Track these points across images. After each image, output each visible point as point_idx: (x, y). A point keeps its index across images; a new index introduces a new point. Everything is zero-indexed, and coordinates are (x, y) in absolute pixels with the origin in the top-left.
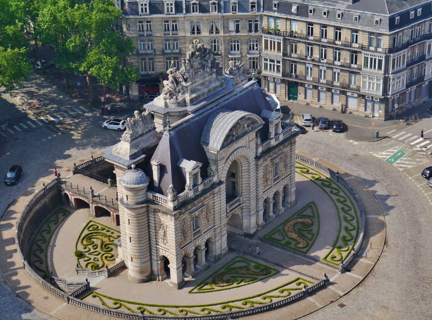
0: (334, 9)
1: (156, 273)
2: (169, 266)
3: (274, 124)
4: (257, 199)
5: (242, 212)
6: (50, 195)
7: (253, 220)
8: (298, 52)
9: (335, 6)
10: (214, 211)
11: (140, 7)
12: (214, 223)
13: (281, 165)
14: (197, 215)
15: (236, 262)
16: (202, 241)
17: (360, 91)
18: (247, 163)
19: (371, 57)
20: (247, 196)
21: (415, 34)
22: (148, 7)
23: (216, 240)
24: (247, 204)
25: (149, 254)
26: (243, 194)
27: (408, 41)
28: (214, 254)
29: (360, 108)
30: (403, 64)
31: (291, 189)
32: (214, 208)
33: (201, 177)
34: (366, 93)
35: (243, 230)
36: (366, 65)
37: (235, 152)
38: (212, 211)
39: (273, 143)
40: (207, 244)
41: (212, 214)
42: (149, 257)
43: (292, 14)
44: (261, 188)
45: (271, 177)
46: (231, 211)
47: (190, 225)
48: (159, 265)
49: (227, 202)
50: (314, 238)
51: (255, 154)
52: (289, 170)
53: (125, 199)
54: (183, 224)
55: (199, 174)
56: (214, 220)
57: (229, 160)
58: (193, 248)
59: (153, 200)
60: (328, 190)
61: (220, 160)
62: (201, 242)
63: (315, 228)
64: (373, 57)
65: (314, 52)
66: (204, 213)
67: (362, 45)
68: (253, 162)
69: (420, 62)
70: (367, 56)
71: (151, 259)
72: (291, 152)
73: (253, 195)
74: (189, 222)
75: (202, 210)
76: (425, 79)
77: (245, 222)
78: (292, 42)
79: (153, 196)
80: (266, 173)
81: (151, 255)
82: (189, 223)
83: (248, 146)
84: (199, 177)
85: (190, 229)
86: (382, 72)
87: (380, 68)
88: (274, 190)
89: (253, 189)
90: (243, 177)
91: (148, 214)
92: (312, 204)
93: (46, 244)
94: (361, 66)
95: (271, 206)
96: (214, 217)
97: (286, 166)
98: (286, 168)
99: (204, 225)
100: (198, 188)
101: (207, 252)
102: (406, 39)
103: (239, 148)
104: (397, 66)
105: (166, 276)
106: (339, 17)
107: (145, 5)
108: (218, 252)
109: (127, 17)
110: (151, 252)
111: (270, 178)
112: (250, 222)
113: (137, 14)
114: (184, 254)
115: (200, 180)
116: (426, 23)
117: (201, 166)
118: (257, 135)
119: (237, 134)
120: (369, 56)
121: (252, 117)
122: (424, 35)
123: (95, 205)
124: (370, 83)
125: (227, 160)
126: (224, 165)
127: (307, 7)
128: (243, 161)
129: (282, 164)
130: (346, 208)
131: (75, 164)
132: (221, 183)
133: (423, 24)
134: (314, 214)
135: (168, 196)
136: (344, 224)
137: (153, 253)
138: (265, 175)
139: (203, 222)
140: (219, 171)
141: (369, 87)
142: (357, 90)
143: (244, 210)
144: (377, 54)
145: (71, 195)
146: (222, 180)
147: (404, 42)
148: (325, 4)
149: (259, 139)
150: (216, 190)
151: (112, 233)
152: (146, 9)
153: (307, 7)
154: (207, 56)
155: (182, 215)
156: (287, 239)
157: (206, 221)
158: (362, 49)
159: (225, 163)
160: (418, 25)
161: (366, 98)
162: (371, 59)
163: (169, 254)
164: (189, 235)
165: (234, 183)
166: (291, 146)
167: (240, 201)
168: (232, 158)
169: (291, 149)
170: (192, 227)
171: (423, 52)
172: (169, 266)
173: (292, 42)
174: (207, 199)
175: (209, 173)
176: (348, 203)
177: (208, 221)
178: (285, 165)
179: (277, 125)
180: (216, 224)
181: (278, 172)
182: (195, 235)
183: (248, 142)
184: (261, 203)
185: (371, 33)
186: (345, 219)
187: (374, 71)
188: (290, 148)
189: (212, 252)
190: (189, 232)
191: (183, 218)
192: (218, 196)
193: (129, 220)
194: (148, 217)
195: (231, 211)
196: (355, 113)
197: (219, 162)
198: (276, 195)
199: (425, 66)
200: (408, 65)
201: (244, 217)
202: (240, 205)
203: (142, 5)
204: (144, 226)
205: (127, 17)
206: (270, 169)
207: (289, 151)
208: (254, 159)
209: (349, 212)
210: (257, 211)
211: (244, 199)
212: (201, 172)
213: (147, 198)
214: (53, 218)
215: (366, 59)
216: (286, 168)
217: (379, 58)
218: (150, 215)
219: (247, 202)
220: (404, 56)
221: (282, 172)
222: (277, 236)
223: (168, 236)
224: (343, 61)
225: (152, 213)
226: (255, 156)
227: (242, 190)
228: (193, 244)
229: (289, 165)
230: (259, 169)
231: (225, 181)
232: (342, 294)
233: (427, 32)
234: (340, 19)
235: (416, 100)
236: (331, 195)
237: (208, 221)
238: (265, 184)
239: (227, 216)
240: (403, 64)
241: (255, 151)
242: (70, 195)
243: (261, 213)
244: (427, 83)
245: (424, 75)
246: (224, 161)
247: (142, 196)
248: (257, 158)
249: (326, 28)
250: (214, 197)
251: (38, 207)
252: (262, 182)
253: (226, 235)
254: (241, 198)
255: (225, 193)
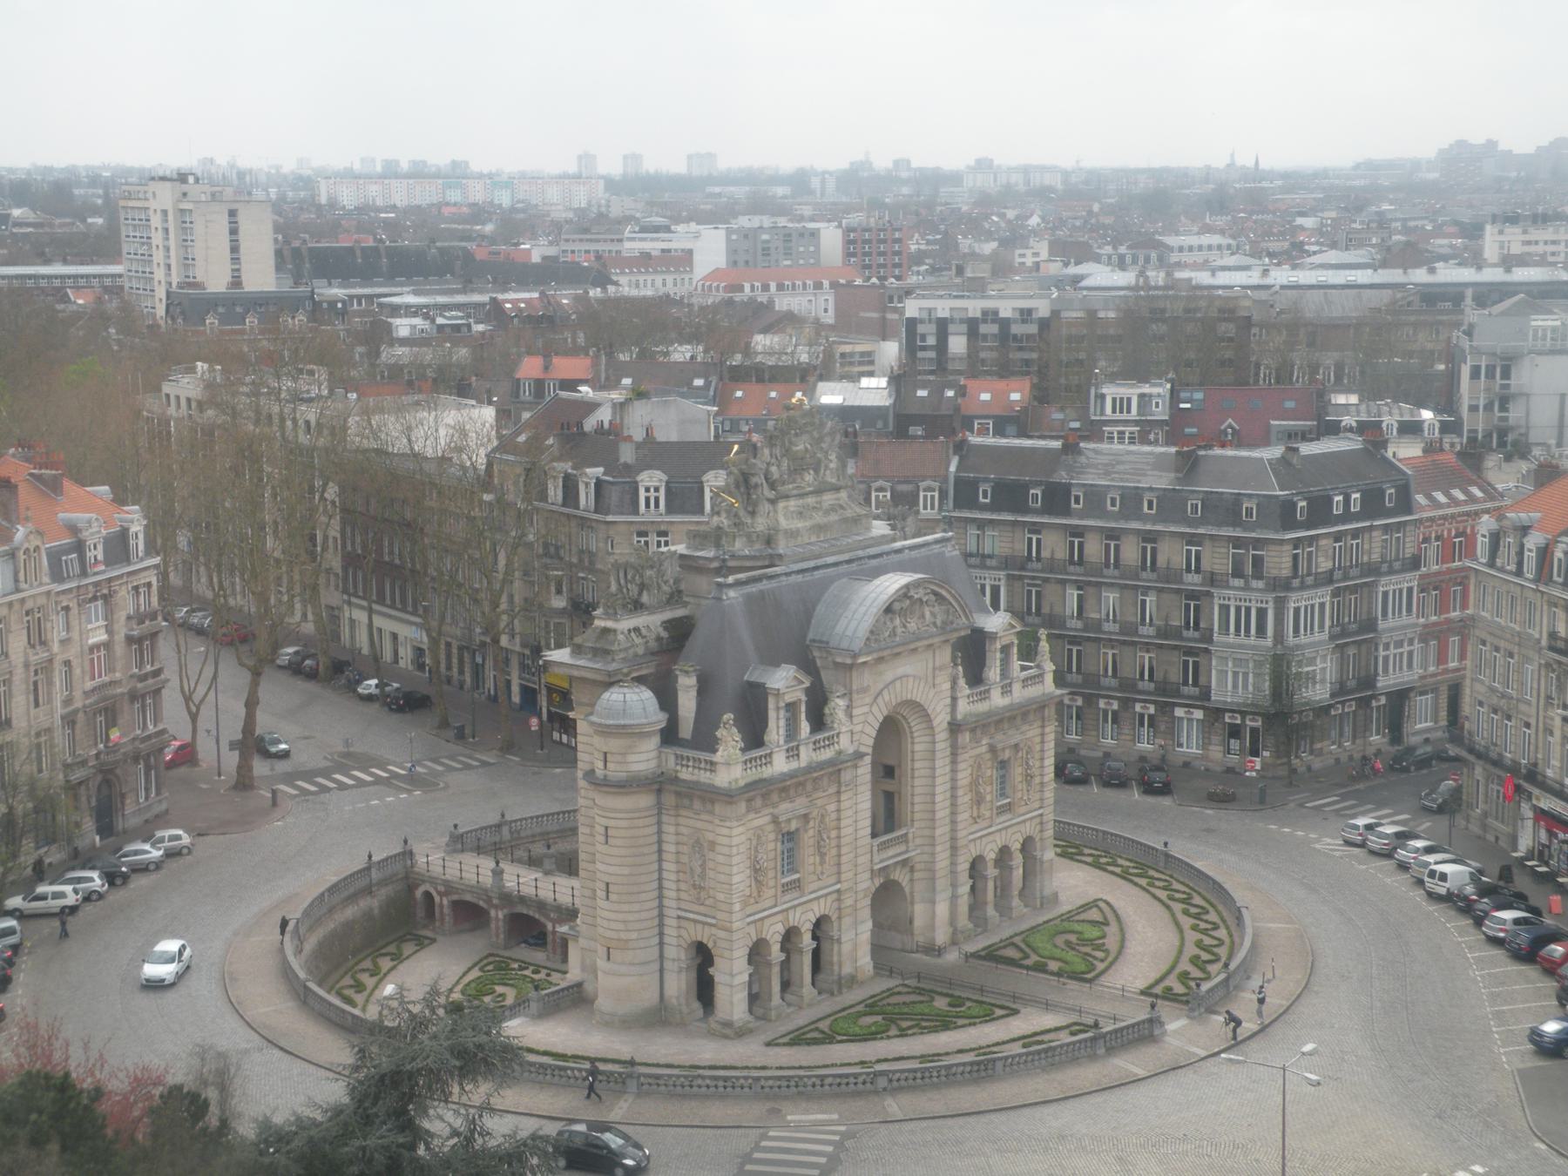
0: (1137, 488)
1: (674, 1001)
2: (711, 971)
3: (998, 646)
4: (954, 849)
5: (911, 880)
6: (384, 893)
7: (942, 909)
8: (1046, 610)
9: (1139, 482)
10: (839, 837)
11: (642, 494)
12: (839, 873)
13: (1017, 771)
14: (794, 826)
15: (899, 993)
16: (803, 918)
17: (1209, 699)
18: (927, 732)
19: (1238, 603)
20: (927, 832)
21: (1348, 558)
22: (662, 494)
23: (843, 927)
24: (926, 858)
25: (656, 940)
26: (916, 824)
27: (1331, 572)
28: (836, 968)
29: (1211, 748)
30: (1322, 626)
31: (1043, 849)
32: (839, 828)
33: (808, 719)
34: (1226, 702)
35: (912, 934)
36: (1225, 629)
37: (898, 684)
38: (833, 834)
39: (998, 700)
40: (819, 925)
41: (834, 843)
42: (657, 948)
43: (1026, 510)
44: (963, 816)
45: (989, 792)
46: (881, 861)
47: (772, 855)
48: (683, 976)
49: (874, 835)
50: (1110, 959)
51: (948, 710)
52: (1037, 796)
53: (600, 764)
54: (754, 842)
55: (803, 708)
56: (839, 864)
57: (880, 700)
58: (780, 928)
59: (677, 771)
60: (1143, 882)
61: (858, 692)
62: (804, 920)
63: (1111, 942)
64: (1243, 603)
65: (1087, 606)
66: (811, 833)
67: (1212, 573)
68: (942, 735)
69: (1363, 634)
70: (1226, 602)
71: (661, 956)
72: (1043, 742)
73: (942, 831)
74: (772, 847)
75: (806, 818)
76: (1379, 685)
77: (919, 910)
78: (1029, 585)
79: (677, 756)
80: (977, 779)
81: (661, 944)
82: (771, 846)
83: (930, 679)
84: (803, 716)
85: (772, 864)
86: (1269, 642)
87: (1261, 630)
88: (1000, 841)
89: (942, 813)
90: (917, 773)
91: (659, 814)
92: (1102, 905)
93: (366, 993)
94: (1212, 630)
95: (991, 885)
96: (839, 856)
97: (1028, 778)
98: (1029, 784)
99: (812, 868)
100: (797, 747)
101: (816, 954)
102: (1324, 565)
103: (908, 676)
104: (1305, 630)
105: (700, 1012)
106: (1150, 507)
107: (657, 490)
108: (847, 969)
109: (610, 518)
110: (661, 925)
111: (988, 798)
112: (934, 912)
113: (636, 512)
114: (755, 939)
115: (805, 727)
116: (1375, 534)
117: (807, 684)
118: (954, 659)
119: (905, 626)
120: (1232, 603)
121: (944, 593)
122: (1369, 564)
123: (505, 911)
124: (1235, 674)
125: (876, 698)
126: (866, 709)
127: (1066, 489)
128: (915, 725)
129: (1019, 770)
130: (1193, 910)
131: (456, 826)
132: (859, 756)
133: (1367, 536)
134: (1105, 918)
135: (715, 751)
136: (1191, 936)
137: (667, 940)
138: (974, 784)
139: (808, 857)
140: (855, 720)
141: (1235, 686)
142: (1202, 700)
143: (917, 875)
144: (1254, 596)
145: (440, 894)
146: (863, 749)
147: (1319, 570)
148: (1112, 480)
149: (960, 668)
150: (846, 776)
151: (548, 975)
152: (657, 500)
153: (1066, 489)
154: (828, 439)
155: (752, 816)
156: (1034, 958)
157: (818, 858)
158: (1212, 585)
159: (871, 705)
160: (1356, 534)
161: (1227, 720)
162: (1238, 609)
163: (714, 930)
164: (772, 883)
165: (889, 797)
166: (1043, 727)
167: (907, 842)
168: (889, 699)
169: (1043, 735)
170: (779, 859)
171: (1369, 612)
172: (711, 971)
173: (1029, 585)
174: (821, 794)
175: (828, 720)
176: (1197, 900)
177: (822, 863)
178: (1027, 775)
179: (1006, 649)
180: (844, 877)
181: (1008, 791)
182: (787, 888)
183: (930, 670)
184: (963, 866)
185: (1237, 542)
186: (1195, 928)
187: (1246, 642)
188: (1038, 731)
189: (832, 964)
190: (771, 874)
191: (757, 823)
192: (850, 794)
193: (606, 828)
194: (659, 823)
195: (881, 861)
196: (1196, 763)
197: (855, 696)
198: (1004, 852)
199: (1376, 649)
200: (1332, 637)
201: (917, 897)
202: (907, 852)
203: (647, 490)
204: (646, 850)
205: (610, 518)
206: (989, 772)
207: (1038, 739)
208: (945, 725)
209: (1205, 917)
210: (954, 886)
211: (918, 841)
212: (807, 702)
213: (659, 766)
214: (392, 948)
215: (1225, 609)
216: (1029, 784)
217: (1259, 605)
218: (665, 818)
219: (926, 849)
220: (1322, 605)
221: (1019, 795)
222: (1011, 953)
223: (711, 874)
224: (1161, 623)
225: (672, 812)
226: (948, 718)
227: (913, 812)
228: (780, 917)
229: (1037, 780)
230: (960, 758)
231: (870, 750)
232: (1203, 1053)
233: (1376, 557)
234: (1153, 512)
235: (1358, 741)
236: (1152, 890)
237: (822, 855)
238: (975, 814)
239: (872, 871)
240: (1322, 626)
241: (948, 701)
242: (439, 893)
243: (965, 889)
244: (1383, 700)
245: (1376, 674)
246: (868, 700)
247: (644, 757)
248: (955, 728)
249: (1118, 538)
250: (839, 792)
251: (350, 912)
252: (967, 798)
253: (869, 925)
254: (910, 836)
255: (868, 814)
